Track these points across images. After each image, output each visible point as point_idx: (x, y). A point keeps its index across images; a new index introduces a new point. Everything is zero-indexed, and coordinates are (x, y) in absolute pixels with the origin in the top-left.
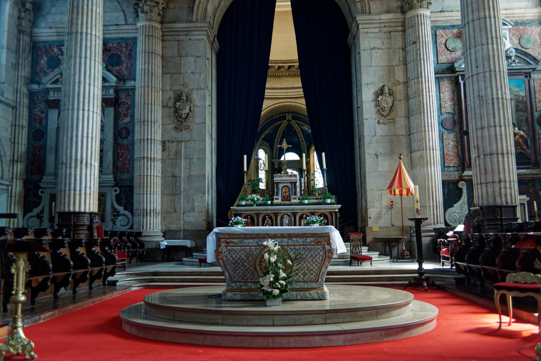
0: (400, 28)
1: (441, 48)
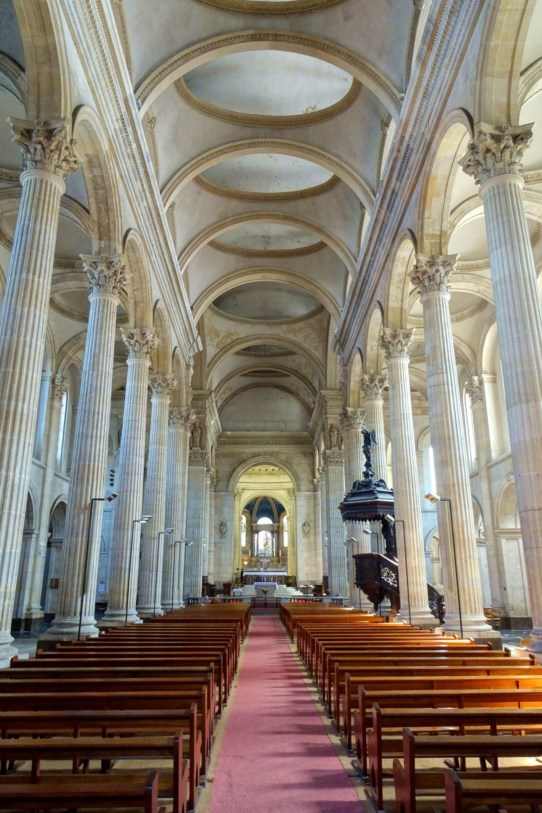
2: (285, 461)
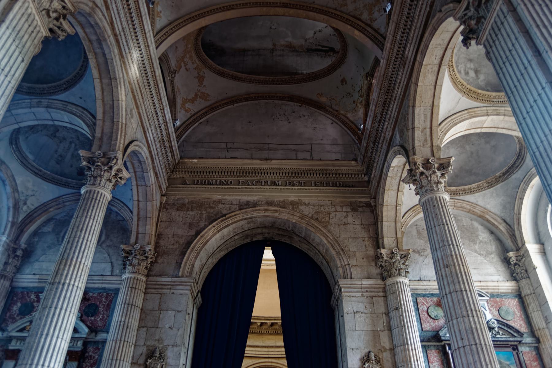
0: (381, 294)
1: (424, 316)
2: (312, 217)
